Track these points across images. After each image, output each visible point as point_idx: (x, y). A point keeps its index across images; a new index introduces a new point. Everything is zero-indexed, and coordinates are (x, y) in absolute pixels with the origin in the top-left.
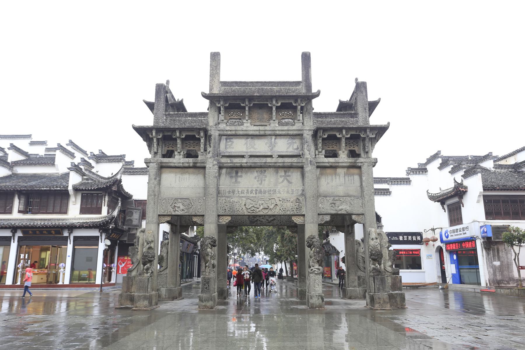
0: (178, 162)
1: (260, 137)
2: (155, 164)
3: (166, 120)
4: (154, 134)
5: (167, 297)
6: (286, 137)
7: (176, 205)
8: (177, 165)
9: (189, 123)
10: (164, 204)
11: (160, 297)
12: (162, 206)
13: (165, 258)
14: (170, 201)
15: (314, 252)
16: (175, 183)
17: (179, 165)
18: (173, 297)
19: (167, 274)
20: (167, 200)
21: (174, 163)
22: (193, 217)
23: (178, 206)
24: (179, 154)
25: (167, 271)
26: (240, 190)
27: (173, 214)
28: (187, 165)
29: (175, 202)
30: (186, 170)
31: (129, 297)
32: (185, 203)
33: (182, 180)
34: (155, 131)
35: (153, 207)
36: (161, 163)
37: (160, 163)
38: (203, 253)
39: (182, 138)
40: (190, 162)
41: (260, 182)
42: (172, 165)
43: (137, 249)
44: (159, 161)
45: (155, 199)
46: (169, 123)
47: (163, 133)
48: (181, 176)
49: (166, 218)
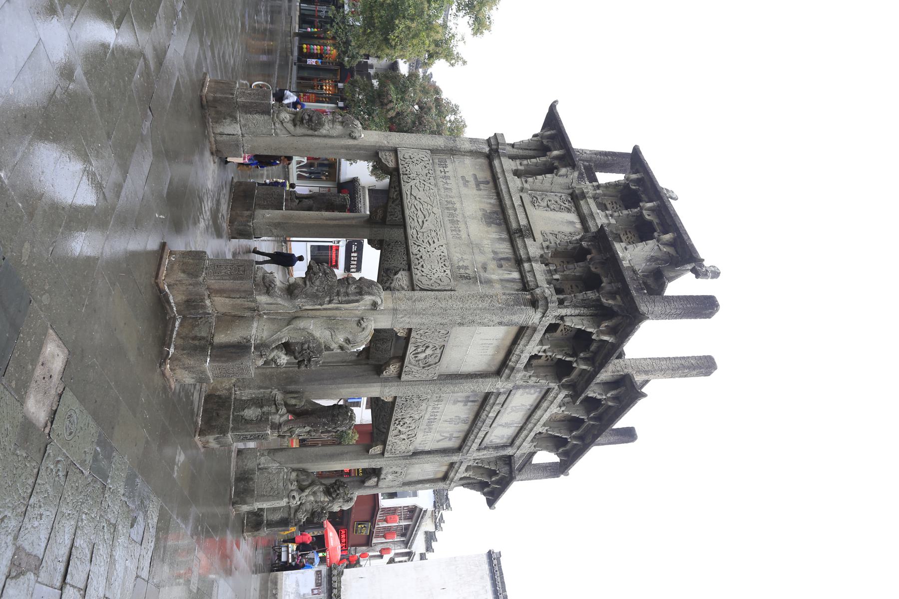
1: (527, 415)
5: (219, 138)
6: (515, 433)
11: (216, 122)
13: (316, 133)
15: (321, 502)
18: (220, 151)
19: (277, 134)
21: (525, 346)
22: (398, 365)
25: (283, 136)
26: (439, 406)
28: (514, 358)
31: (198, 297)
38: (320, 427)
40: (518, 365)
41: (449, 420)
43: (330, 302)
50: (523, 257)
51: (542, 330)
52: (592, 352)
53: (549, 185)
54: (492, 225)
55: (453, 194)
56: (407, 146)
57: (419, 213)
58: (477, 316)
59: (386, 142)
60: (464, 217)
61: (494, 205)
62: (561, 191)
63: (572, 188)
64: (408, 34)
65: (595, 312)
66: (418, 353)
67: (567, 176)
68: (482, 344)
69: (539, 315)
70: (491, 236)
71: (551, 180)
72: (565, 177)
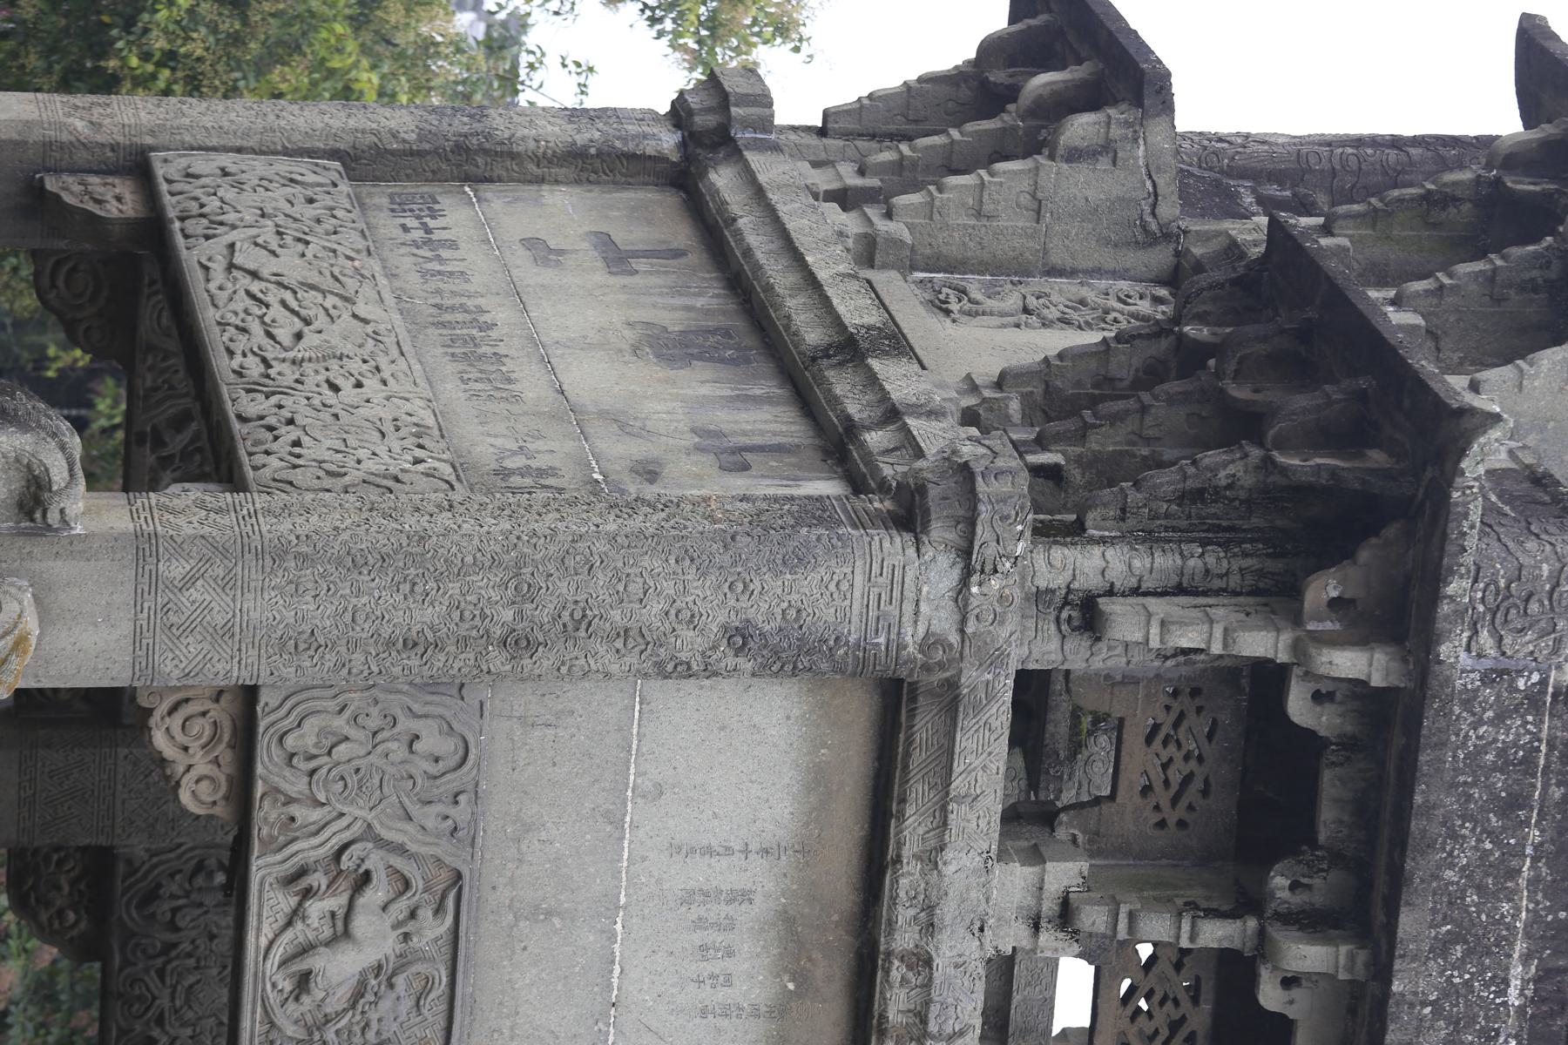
0: (947, 911)
2: (942, 620)
3: (1533, 700)
4: (1346, 663)
7: (375, 895)
8: (907, 879)
9: (1450, 991)
10: (398, 750)
12: (373, 723)
14: (429, 816)
16: (675, 849)
17: (904, 914)
20: (452, 782)
21: (932, 858)
23: (360, 924)
24: (1049, 907)
27: (263, 869)
29: (417, 883)
30: (831, 975)
32: (391, 1011)
33: (700, 924)
34: (1377, 681)
35: (364, 630)
36: (951, 700)
37: (952, 685)
39: (1253, 980)
42: (912, 830)
44: (972, 677)
45: (463, 642)
46: (1481, 751)
47: (1349, 744)
48: (760, 908)
49: (202, 768)
50: (853, 409)
51: (991, 697)
52: (1337, 858)
53: (1024, 222)
54: (694, 362)
55: (472, 288)
56: (201, 139)
57: (276, 311)
58: (602, 578)
59: (80, 125)
60: (534, 342)
61: (707, 312)
62: (1108, 259)
63: (1167, 235)
64: (236, 39)
65: (1271, 565)
66: (306, 950)
67: (1106, 149)
68: (688, 898)
69: (941, 574)
70: (690, 392)
71: (1026, 185)
72: (1104, 163)
